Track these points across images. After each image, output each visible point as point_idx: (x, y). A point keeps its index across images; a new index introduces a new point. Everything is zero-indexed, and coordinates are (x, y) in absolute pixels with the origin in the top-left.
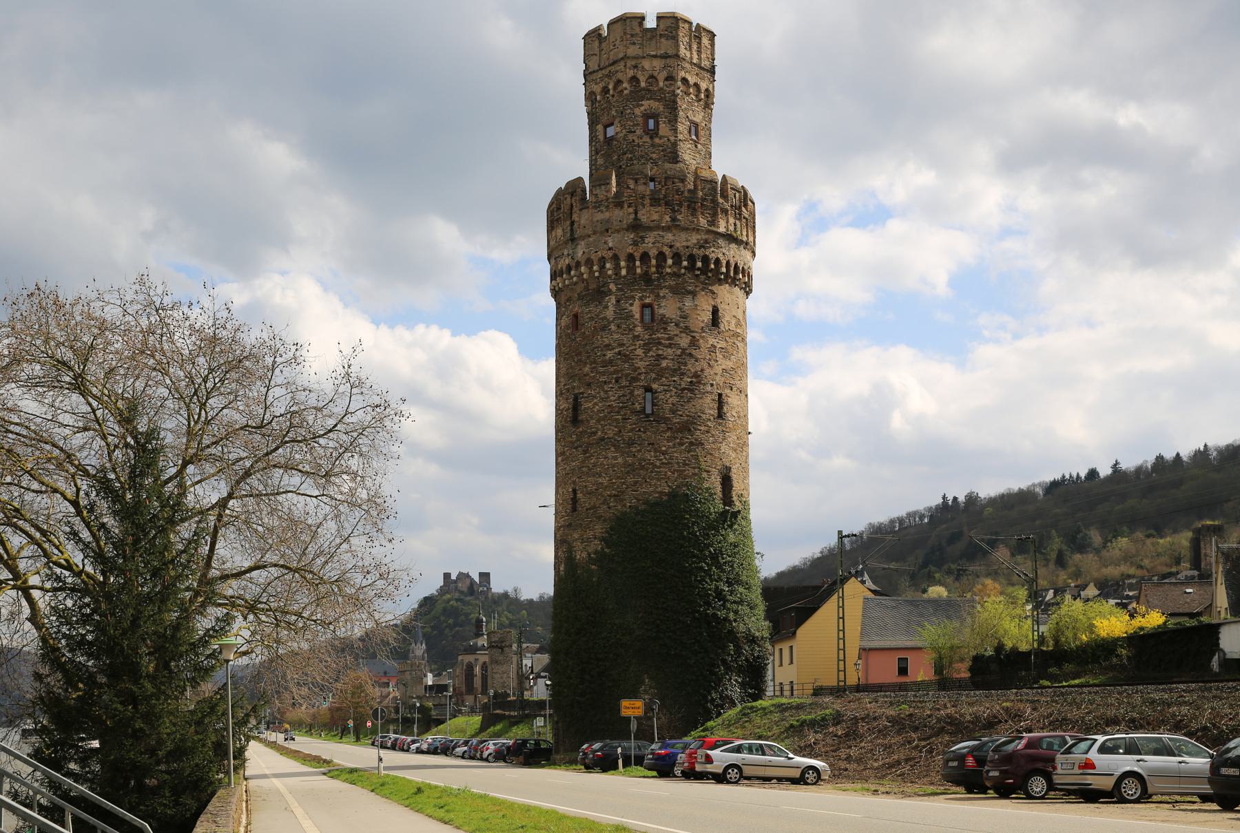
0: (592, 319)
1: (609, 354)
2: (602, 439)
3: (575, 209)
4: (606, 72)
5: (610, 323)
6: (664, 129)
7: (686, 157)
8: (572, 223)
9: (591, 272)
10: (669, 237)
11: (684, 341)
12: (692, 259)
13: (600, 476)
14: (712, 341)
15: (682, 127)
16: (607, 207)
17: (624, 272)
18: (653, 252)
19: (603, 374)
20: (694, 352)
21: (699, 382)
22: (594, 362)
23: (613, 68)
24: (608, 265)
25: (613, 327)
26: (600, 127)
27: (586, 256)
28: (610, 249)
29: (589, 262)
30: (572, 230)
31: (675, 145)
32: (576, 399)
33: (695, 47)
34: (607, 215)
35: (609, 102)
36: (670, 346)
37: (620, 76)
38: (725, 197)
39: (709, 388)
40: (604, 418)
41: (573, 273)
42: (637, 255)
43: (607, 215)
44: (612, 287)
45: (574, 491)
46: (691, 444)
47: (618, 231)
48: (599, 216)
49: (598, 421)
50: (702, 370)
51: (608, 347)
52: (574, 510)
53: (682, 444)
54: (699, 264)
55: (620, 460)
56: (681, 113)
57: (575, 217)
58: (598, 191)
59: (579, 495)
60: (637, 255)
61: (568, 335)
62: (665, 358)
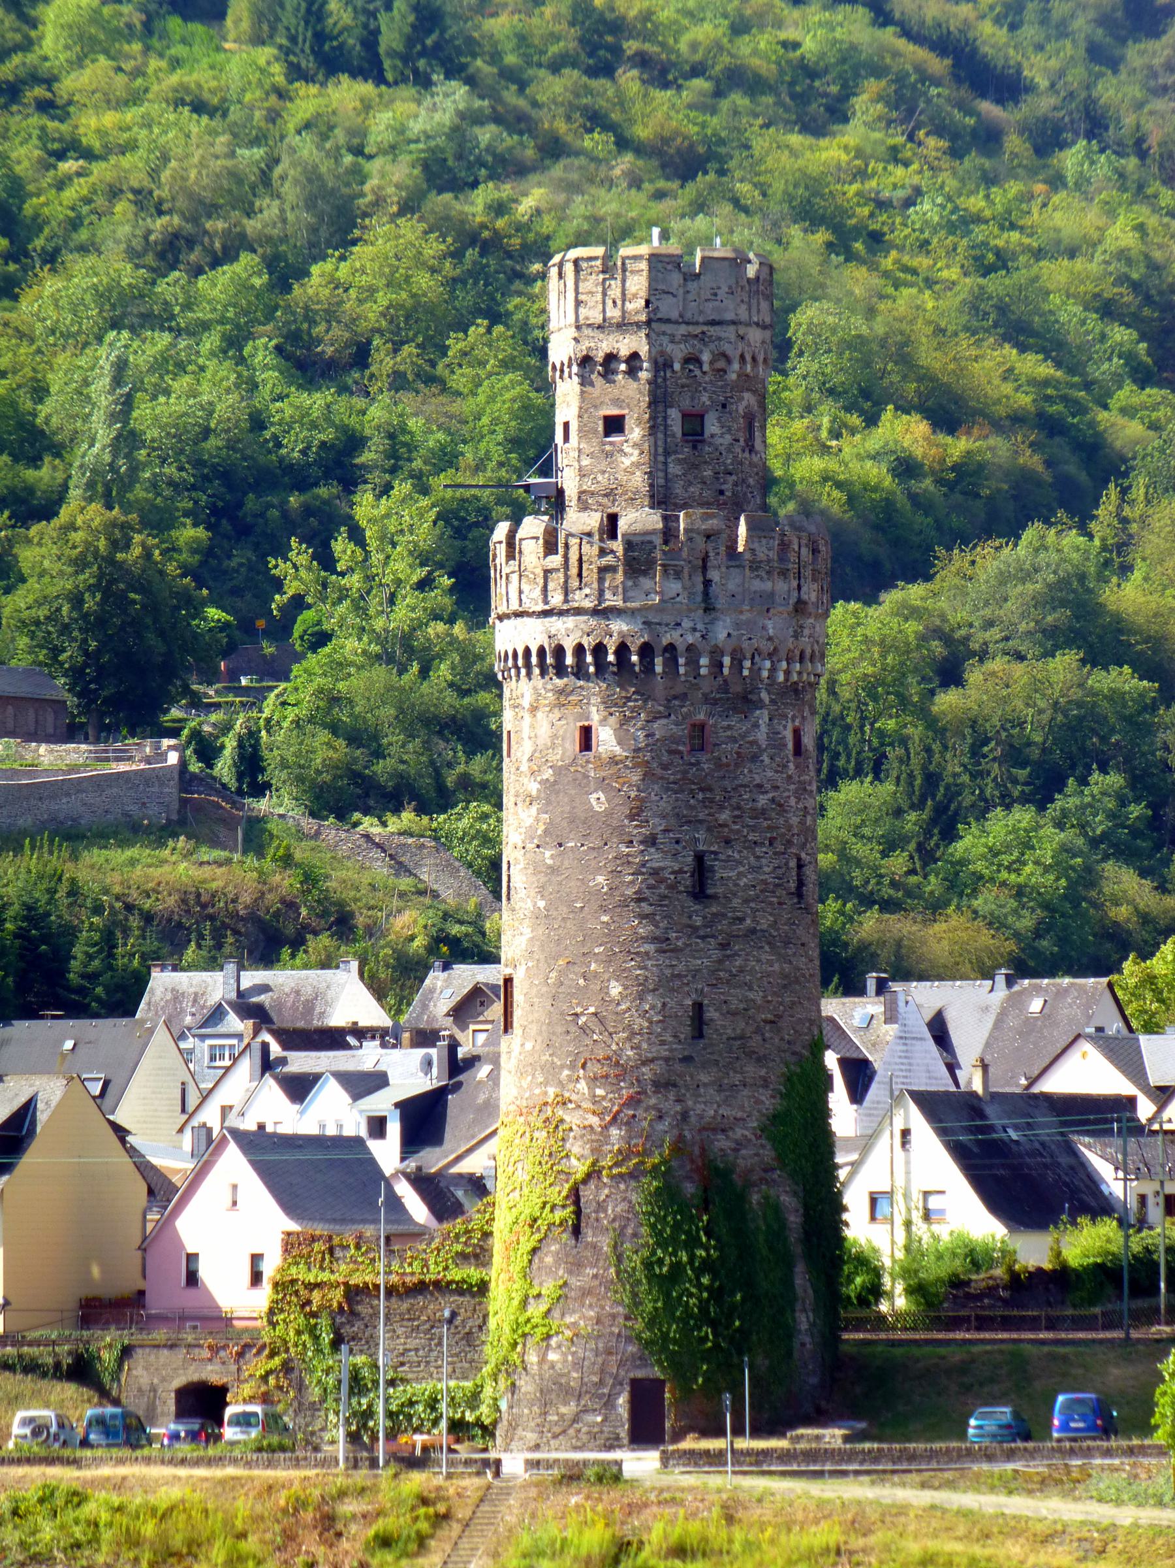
1: (763, 800)
2: (753, 931)
4: (697, 330)
5: (762, 751)
13: (751, 989)
19: (753, 829)
22: (739, 808)
23: (712, 331)
27: (732, 643)
28: (770, 639)
34: (768, 586)
37: (727, 348)
43: (768, 586)
44: (764, 695)
48: (757, 585)
49: (746, 901)
52: (699, 1034)
55: (776, 967)
58: (756, 545)
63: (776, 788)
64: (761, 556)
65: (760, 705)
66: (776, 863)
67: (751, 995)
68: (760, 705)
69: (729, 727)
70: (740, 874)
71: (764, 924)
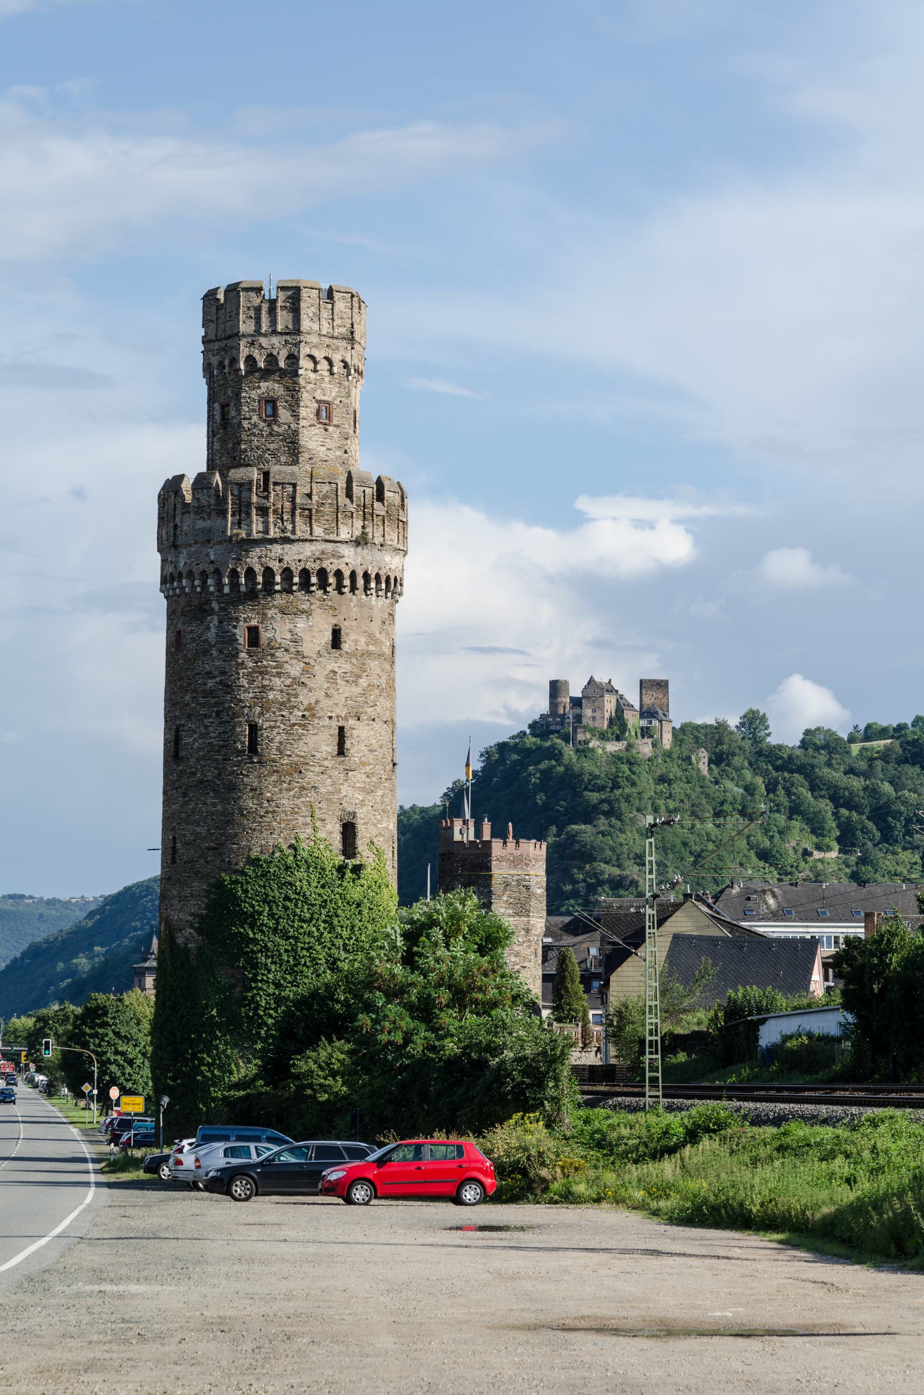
0: (193, 640)
1: (211, 683)
2: (201, 782)
3: (178, 512)
5: (211, 646)
6: (284, 415)
7: (311, 445)
8: (176, 526)
9: (193, 587)
10: (277, 549)
11: (295, 669)
12: (305, 573)
13: (198, 825)
14: (333, 666)
15: (307, 411)
16: (209, 514)
17: (227, 590)
18: (258, 569)
19: (204, 705)
20: (306, 681)
21: (313, 715)
22: (195, 691)
24: (210, 581)
25: (214, 652)
26: (217, 406)
27: (188, 568)
28: (212, 562)
29: (190, 575)
30: (175, 535)
31: (296, 433)
32: (177, 731)
33: (325, 314)
34: (208, 524)
36: (279, 675)
38: (349, 494)
39: (327, 722)
40: (203, 758)
41: (175, 584)
42: (242, 571)
43: (208, 524)
44: (215, 605)
45: (174, 838)
46: (303, 788)
47: (220, 543)
48: (201, 524)
49: (198, 760)
50: (317, 702)
51: (209, 675)
53: (289, 790)
54: (314, 580)
55: (219, 807)
56: (305, 395)
57: (178, 520)
59: (179, 845)
60: (242, 571)
61: (172, 654)
63: (224, 673)
64: (204, 503)
65: (211, 612)
66: (222, 729)
68: (211, 612)
69: (192, 632)
70: (195, 740)
71: (210, 775)
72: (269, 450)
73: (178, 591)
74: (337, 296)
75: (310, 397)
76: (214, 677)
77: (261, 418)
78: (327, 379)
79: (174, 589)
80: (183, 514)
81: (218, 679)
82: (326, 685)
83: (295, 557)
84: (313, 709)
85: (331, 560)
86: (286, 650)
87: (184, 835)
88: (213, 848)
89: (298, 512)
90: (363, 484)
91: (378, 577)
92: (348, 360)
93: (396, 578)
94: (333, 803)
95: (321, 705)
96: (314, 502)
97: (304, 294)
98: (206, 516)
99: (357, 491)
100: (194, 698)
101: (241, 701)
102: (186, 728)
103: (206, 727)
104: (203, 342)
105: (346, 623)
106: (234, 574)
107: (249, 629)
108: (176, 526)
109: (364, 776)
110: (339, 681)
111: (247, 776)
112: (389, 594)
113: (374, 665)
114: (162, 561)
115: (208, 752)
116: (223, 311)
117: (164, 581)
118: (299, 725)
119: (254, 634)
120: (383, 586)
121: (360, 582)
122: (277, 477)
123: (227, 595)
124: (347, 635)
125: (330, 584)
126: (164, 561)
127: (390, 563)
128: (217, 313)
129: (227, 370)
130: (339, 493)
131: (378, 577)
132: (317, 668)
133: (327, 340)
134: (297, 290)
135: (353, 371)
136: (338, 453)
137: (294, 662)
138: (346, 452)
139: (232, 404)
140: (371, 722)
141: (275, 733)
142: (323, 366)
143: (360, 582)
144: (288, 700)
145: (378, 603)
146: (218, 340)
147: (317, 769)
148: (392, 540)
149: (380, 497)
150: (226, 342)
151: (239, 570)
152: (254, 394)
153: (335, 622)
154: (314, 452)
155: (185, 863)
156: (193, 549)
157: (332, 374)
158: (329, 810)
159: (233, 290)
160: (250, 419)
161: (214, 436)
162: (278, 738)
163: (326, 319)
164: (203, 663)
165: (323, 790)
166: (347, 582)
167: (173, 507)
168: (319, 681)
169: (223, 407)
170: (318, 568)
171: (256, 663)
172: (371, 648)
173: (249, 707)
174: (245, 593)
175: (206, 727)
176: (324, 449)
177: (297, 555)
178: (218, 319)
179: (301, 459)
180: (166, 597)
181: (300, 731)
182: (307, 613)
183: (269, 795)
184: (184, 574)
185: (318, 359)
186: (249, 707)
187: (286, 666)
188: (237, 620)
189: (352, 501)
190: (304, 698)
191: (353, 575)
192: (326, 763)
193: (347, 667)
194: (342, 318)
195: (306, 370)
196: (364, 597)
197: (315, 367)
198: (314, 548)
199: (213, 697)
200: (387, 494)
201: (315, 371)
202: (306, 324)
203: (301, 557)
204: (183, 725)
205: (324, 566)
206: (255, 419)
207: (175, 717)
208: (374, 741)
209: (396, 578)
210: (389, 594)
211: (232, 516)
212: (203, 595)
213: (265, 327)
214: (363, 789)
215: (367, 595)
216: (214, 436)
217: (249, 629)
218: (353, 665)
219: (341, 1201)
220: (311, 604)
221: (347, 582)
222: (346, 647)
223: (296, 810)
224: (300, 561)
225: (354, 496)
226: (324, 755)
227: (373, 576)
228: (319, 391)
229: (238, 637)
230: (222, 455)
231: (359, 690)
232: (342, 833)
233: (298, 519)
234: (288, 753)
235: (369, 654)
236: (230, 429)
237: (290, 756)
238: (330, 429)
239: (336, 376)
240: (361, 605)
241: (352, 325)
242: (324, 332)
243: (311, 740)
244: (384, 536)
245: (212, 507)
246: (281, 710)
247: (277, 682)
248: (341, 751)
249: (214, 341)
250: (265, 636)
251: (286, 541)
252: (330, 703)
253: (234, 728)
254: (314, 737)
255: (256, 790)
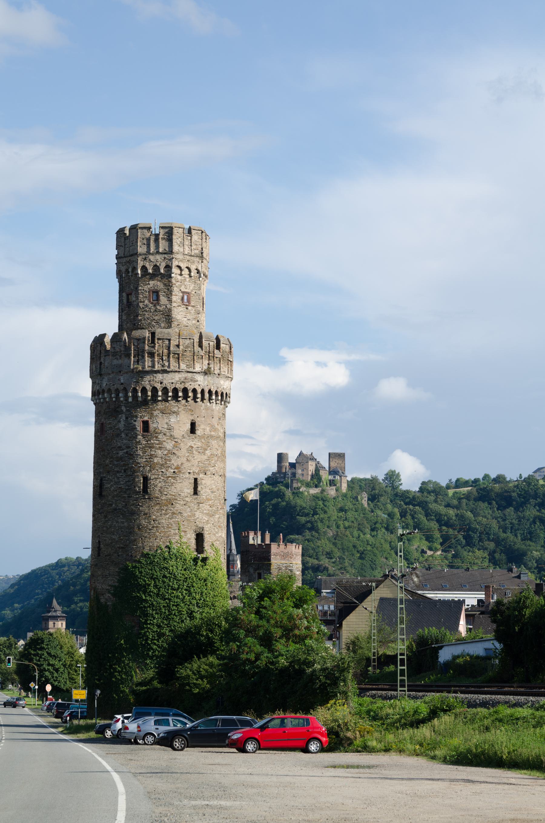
0: (111, 428)
1: (121, 453)
2: (115, 509)
5: (121, 432)
6: (163, 300)
8: (101, 363)
9: (111, 398)
10: (159, 377)
12: (175, 390)
13: (113, 534)
15: (176, 298)
17: (130, 400)
18: (149, 388)
21: (180, 472)
22: (112, 458)
24: (121, 395)
25: (123, 435)
26: (124, 294)
28: (122, 384)
29: (109, 391)
30: (100, 368)
31: (170, 310)
32: (101, 480)
33: (187, 243)
34: (120, 362)
35: (129, 279)
36: (160, 448)
38: (201, 345)
39: (187, 475)
41: (100, 396)
42: (139, 389)
43: (120, 362)
44: (124, 408)
45: (99, 542)
46: (173, 513)
47: (127, 373)
48: (115, 362)
49: (113, 497)
50: (182, 464)
53: (166, 514)
54: (180, 394)
55: (126, 524)
58: (115, 346)
59: (102, 546)
60: (139, 389)
62: (156, 457)
64: (117, 350)
65: (121, 412)
66: (127, 479)
67: (113, 537)
68: (121, 412)
69: (110, 424)
70: (112, 486)
71: (120, 506)
72: (154, 320)
73: (102, 400)
74: (193, 232)
75: (178, 290)
76: (123, 450)
77: (150, 301)
78: (188, 280)
79: (100, 399)
80: (105, 356)
81: (125, 451)
82: (187, 454)
83: (170, 381)
84: (179, 468)
85: (190, 383)
86: (165, 434)
87: (105, 540)
88: (122, 548)
89: (171, 355)
90: (208, 339)
91: (216, 392)
92: (200, 268)
93: (226, 394)
94: (191, 522)
95: (185, 466)
96: (181, 349)
97: (175, 231)
98: (118, 357)
99: (205, 343)
100: (112, 461)
101: (138, 463)
102: (106, 479)
103: (118, 478)
104: (117, 258)
105: (198, 419)
106: (135, 391)
107: (143, 422)
108: (101, 363)
109: (208, 506)
110: (194, 452)
111: (142, 506)
112: (223, 403)
113: (214, 443)
114: (93, 383)
115: (119, 492)
116: (128, 240)
117: (94, 394)
118: (172, 477)
119: (146, 425)
120: (220, 398)
121: (207, 396)
122: (160, 335)
123: (131, 402)
124: (199, 426)
125: (189, 397)
126: (94, 383)
127: (223, 385)
128: (125, 242)
129: (130, 274)
130: (195, 345)
131: (216, 392)
132: (182, 444)
133: (188, 257)
134: (171, 228)
135: (202, 275)
136: (194, 322)
137: (169, 441)
138: (198, 321)
139: (133, 294)
140: (212, 476)
141: (158, 482)
142: (186, 272)
143: (207, 396)
144: (166, 463)
145: (216, 407)
146: (125, 257)
147: (182, 502)
148: (224, 372)
149: (218, 347)
150: (130, 258)
151: (137, 388)
152: (146, 288)
153: (192, 418)
154: (180, 321)
155: (106, 556)
156: (111, 376)
157: (190, 277)
158: (188, 526)
159: (134, 228)
160: (144, 302)
161: (122, 312)
162: (160, 485)
163: (187, 245)
164: (116, 441)
165: (185, 515)
166: (199, 395)
167: (99, 352)
168: (183, 452)
169: (128, 295)
170: (183, 387)
171: (147, 441)
172: (213, 433)
173: (143, 467)
174: (141, 402)
175: (118, 478)
176: (186, 319)
177: (171, 380)
178: (125, 245)
179: (173, 325)
180: (95, 404)
181: (172, 481)
182: (176, 413)
183: (154, 517)
184: (106, 391)
185: (182, 268)
186: (143, 467)
187: (164, 443)
188: (136, 417)
189: (202, 349)
190: (175, 462)
191: (203, 392)
192: (187, 499)
193: (199, 444)
194: (196, 245)
195: (176, 274)
196: (209, 404)
197: (181, 273)
198: (180, 376)
199: (122, 461)
200: (222, 345)
201: (181, 275)
202: (176, 248)
203: (173, 381)
204: (105, 477)
205: (186, 386)
206: (147, 302)
207: (100, 472)
208: (214, 487)
209: (226, 394)
210: (223, 403)
211: (134, 357)
212: (117, 403)
213: (152, 250)
214: (207, 514)
215: (210, 403)
216: (122, 312)
217: (143, 422)
218: (203, 443)
219: (234, 750)
220: (179, 408)
221: (199, 395)
222: (199, 432)
223: (170, 526)
224: (172, 383)
225: (204, 346)
226: (186, 494)
227: (214, 392)
228: (183, 286)
229: (137, 427)
230: (128, 323)
231: (205, 457)
232: (196, 539)
233: (171, 359)
234: (165, 493)
235: (212, 436)
236: (132, 308)
237: (166, 495)
238: (190, 308)
239: (192, 278)
240: (207, 409)
241: (202, 249)
242: (186, 253)
243: (178, 486)
244: (220, 369)
245: (122, 352)
246: (161, 468)
247: (159, 452)
248: (196, 492)
249: (123, 258)
250: (152, 426)
251: (165, 372)
252: (190, 465)
253: (134, 479)
254: (180, 484)
255: (147, 514)
